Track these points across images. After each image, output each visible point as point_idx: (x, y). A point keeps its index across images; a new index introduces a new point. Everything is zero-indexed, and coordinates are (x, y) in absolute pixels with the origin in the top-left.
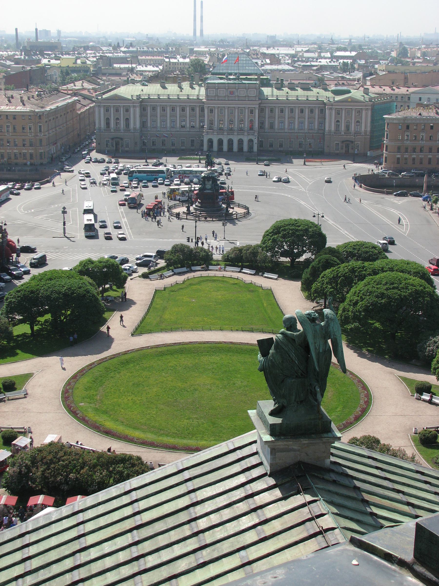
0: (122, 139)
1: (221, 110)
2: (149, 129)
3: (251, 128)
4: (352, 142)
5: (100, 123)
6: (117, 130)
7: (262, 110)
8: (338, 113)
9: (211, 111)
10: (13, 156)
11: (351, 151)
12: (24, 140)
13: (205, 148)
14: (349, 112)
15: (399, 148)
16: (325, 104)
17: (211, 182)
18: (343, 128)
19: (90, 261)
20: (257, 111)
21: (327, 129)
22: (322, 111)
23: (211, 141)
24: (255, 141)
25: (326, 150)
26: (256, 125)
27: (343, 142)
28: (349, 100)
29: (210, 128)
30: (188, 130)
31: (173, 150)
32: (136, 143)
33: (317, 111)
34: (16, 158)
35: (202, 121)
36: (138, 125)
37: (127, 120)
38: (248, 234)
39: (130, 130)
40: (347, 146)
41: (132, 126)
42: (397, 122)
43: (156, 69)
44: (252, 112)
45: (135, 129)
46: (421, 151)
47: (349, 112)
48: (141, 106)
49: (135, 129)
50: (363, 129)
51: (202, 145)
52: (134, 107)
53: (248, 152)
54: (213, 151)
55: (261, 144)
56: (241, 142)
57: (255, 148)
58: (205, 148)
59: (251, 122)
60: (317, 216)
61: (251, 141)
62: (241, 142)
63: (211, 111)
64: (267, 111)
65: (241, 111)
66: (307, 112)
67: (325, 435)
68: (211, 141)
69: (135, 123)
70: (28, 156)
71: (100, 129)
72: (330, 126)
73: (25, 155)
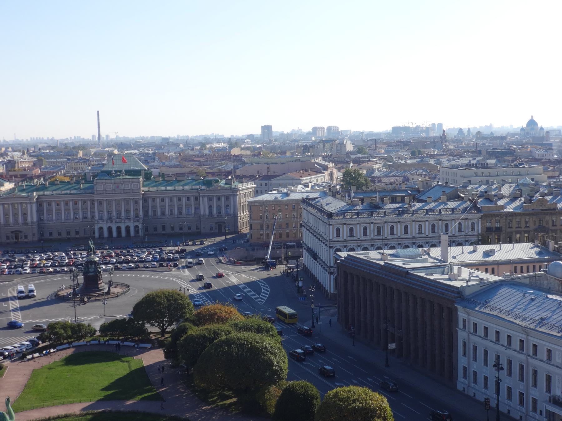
0: (21, 232)
1: (109, 202)
2: (46, 222)
3: (137, 216)
4: (224, 223)
6: (16, 223)
7: (145, 200)
8: (210, 199)
9: (100, 203)
11: (223, 231)
14: (219, 198)
15: (261, 226)
16: (199, 193)
17: (94, 266)
18: (215, 211)
20: (141, 202)
21: (202, 213)
22: (197, 199)
24: (141, 226)
25: (203, 231)
26: (141, 213)
27: (216, 223)
28: (219, 188)
29: (101, 218)
30: (81, 220)
31: (69, 239)
32: (34, 235)
33: (192, 199)
35: (93, 213)
36: (35, 219)
37: (25, 215)
39: (27, 224)
40: (220, 226)
41: (29, 220)
42: (257, 204)
44: (136, 202)
45: (32, 222)
46: (280, 227)
47: (219, 198)
48: (37, 201)
49: (32, 222)
50: (232, 212)
51: (94, 233)
52: (31, 203)
53: (135, 236)
54: (103, 238)
55: (146, 229)
56: (128, 229)
57: (141, 233)
58: (97, 235)
59: (136, 210)
60: (183, 290)
61: (136, 227)
62: (128, 229)
63: (100, 203)
64: (150, 201)
65: (127, 202)
66: (184, 200)
68: (101, 228)
69: (33, 217)
72: (204, 210)
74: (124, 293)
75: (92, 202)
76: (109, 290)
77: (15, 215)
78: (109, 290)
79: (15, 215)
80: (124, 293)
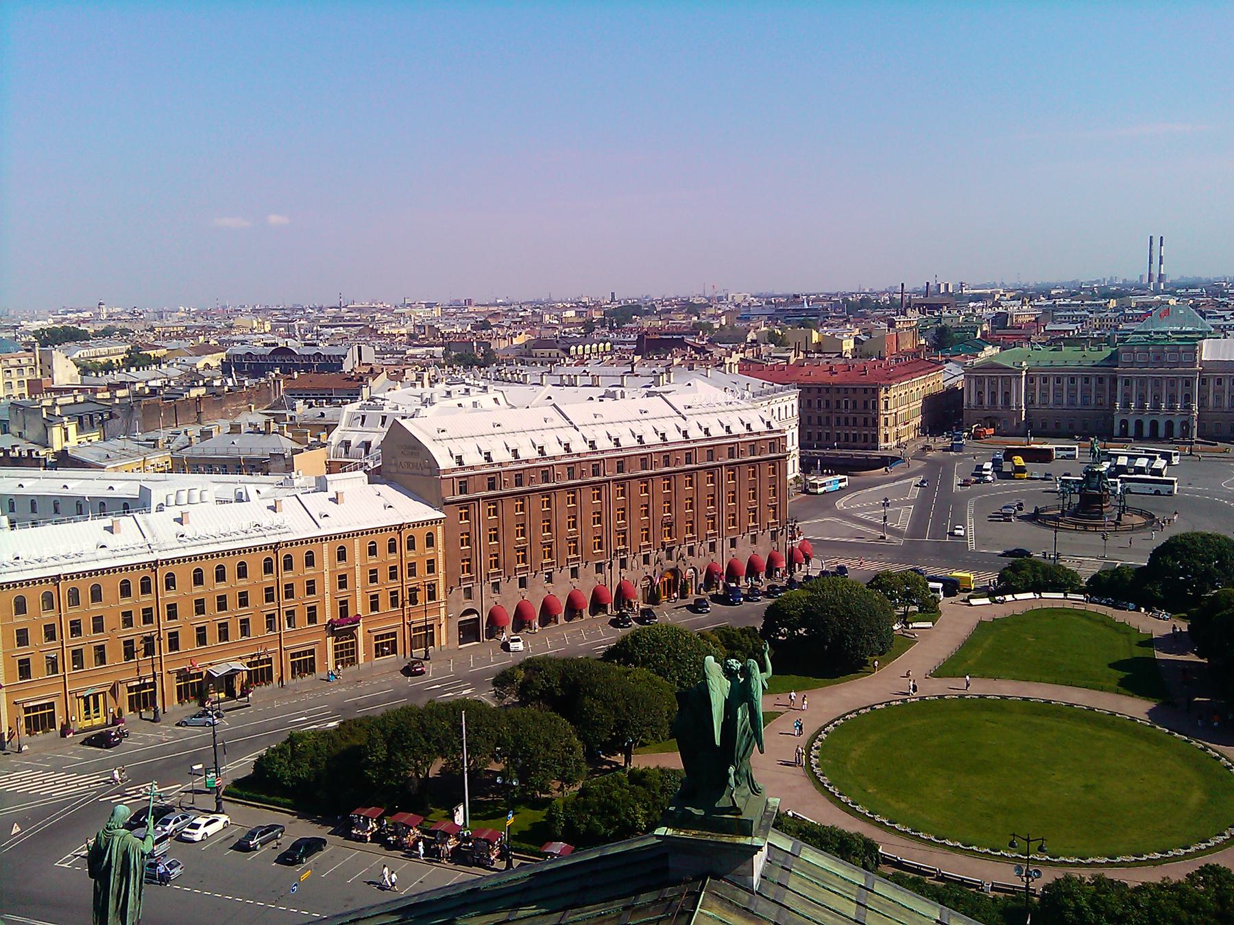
5: (970, 400)
10: (851, 439)
12: (866, 419)
13: (1116, 431)
19: (889, 575)
23: (1124, 422)
34: (855, 441)
35: (1113, 398)
37: (1007, 395)
38: (1134, 552)
43: (1072, 327)
58: (1116, 431)
59: (1188, 398)
67: (742, 840)
68: (1124, 422)
69: (1020, 399)
70: (870, 438)
71: (969, 405)
73: (866, 436)
74: (1145, 526)
75: (1114, 380)
76: (1119, 518)
77: (993, 395)
78: (1119, 518)
79: (993, 395)
80: (1145, 526)
